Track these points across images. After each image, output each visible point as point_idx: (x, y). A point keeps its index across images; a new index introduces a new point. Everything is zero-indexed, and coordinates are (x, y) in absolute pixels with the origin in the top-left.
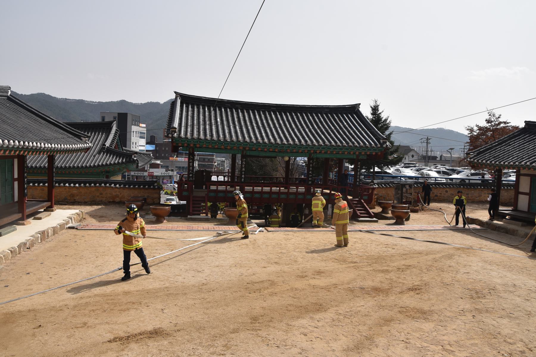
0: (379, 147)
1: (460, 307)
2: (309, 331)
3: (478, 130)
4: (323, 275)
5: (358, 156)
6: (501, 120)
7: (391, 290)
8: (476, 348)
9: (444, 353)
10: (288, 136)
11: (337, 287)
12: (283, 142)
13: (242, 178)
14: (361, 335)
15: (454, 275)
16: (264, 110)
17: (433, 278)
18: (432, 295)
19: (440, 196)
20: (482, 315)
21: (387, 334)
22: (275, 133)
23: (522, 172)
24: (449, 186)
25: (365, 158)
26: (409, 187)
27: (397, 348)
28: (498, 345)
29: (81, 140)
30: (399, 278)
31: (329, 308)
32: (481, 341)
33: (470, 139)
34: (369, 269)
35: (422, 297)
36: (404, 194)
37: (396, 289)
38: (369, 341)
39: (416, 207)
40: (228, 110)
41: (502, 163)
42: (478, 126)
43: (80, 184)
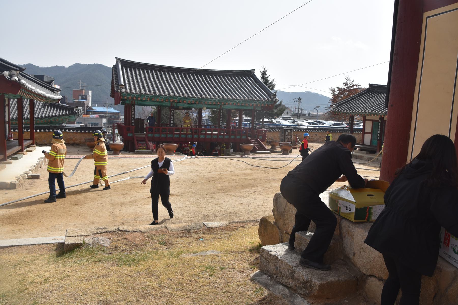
3: (339, 90)
4: (247, 175)
5: (254, 108)
6: (354, 83)
12: (203, 97)
13: (171, 123)
16: (184, 73)
19: (312, 138)
22: (195, 90)
24: (318, 131)
25: (260, 109)
29: (54, 92)
36: (286, 137)
40: (158, 72)
41: (354, 111)
43: (40, 130)
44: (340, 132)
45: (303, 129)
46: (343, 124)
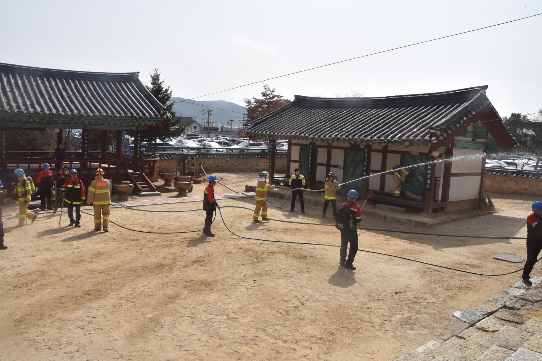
0: (159, 118)
1: (243, 273)
2: (86, 323)
3: (255, 102)
4: (101, 257)
5: (137, 127)
6: (275, 93)
7: (175, 265)
8: (258, 311)
9: (229, 322)
10: (58, 105)
11: (117, 269)
13: (3, 154)
14: (145, 318)
15: (235, 243)
16: (27, 74)
17: (216, 248)
18: (216, 265)
20: (261, 278)
21: (173, 312)
22: (42, 102)
23: (293, 141)
25: (145, 129)
26: (191, 158)
27: (183, 325)
28: (276, 305)
30: (182, 251)
31: (109, 293)
32: (262, 304)
33: (247, 111)
34: (152, 245)
35: (206, 268)
36: (186, 166)
37: (180, 263)
38: (154, 323)
39: (199, 178)
41: (276, 134)
42: (255, 98)
44: (258, 156)
45: (210, 154)
46: (261, 144)
